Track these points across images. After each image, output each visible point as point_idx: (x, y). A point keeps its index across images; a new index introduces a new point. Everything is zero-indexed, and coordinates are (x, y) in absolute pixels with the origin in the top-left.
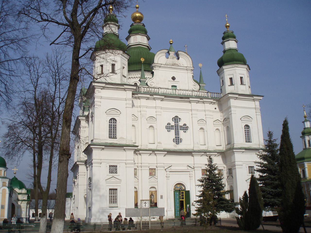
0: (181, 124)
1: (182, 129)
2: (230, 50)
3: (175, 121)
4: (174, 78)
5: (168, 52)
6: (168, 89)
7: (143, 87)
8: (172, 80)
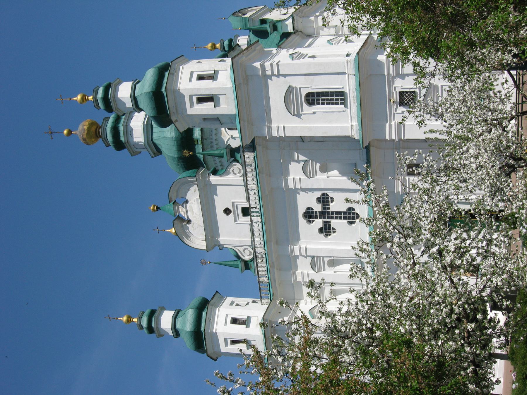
0: (317, 208)
1: (328, 205)
3: (313, 217)
4: (227, 211)
8: (232, 215)
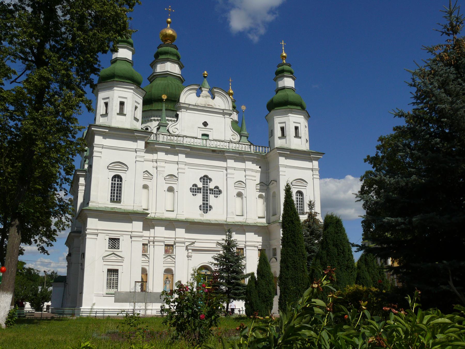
0: (211, 186)
1: (212, 194)
2: (284, 88)
3: (204, 182)
4: (205, 124)
5: (200, 88)
6: (197, 138)
7: (162, 134)
8: (203, 127)
